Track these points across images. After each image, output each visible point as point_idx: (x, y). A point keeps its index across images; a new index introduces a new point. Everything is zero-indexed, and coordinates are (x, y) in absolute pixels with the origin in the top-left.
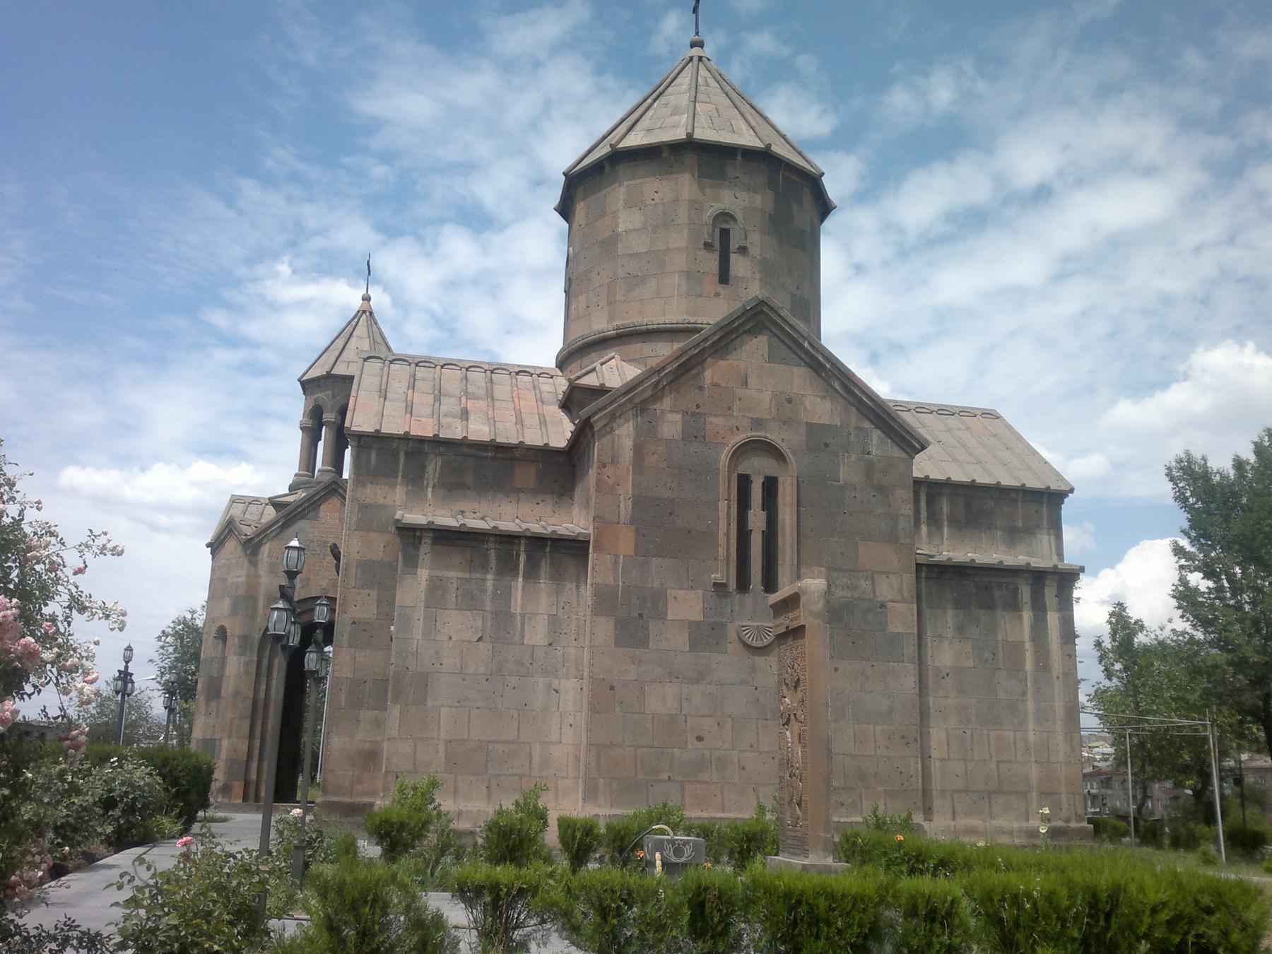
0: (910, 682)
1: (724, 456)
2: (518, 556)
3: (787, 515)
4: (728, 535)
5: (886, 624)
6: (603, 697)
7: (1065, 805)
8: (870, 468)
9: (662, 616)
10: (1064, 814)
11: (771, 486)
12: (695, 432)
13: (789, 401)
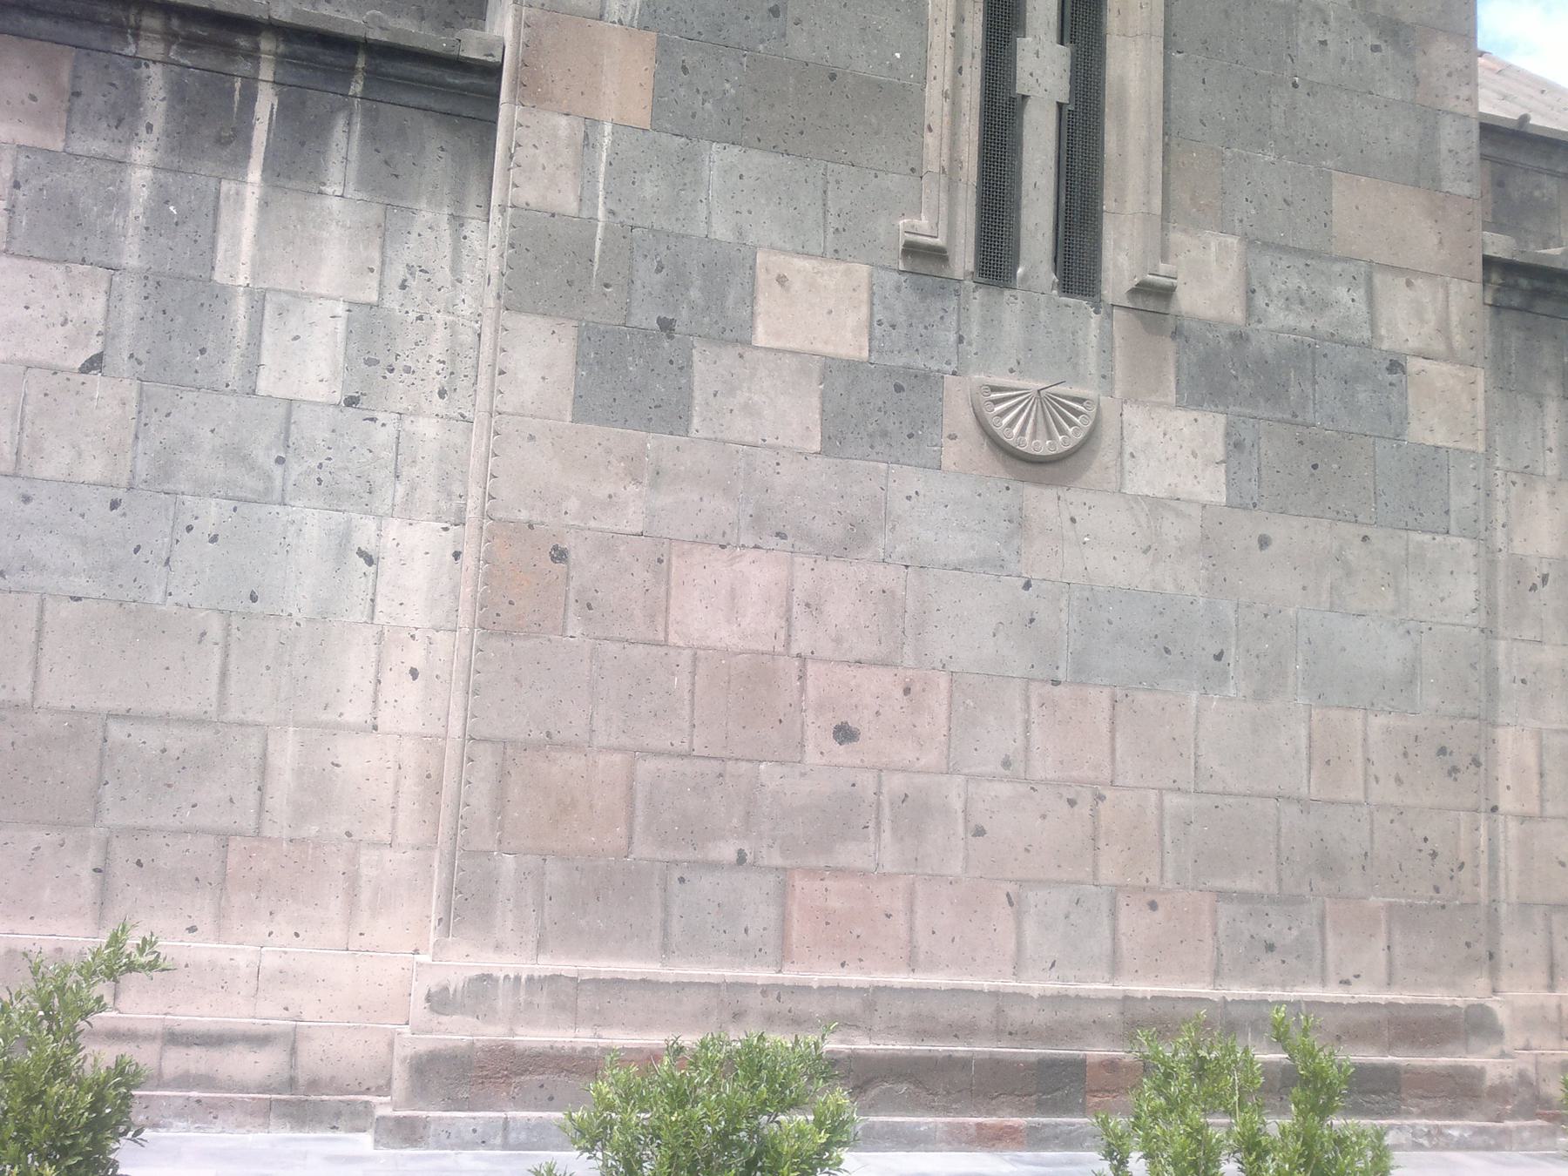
2: (250, 98)
3: (1132, 65)
4: (953, 96)
5: (1404, 418)
6: (523, 584)
9: (736, 335)
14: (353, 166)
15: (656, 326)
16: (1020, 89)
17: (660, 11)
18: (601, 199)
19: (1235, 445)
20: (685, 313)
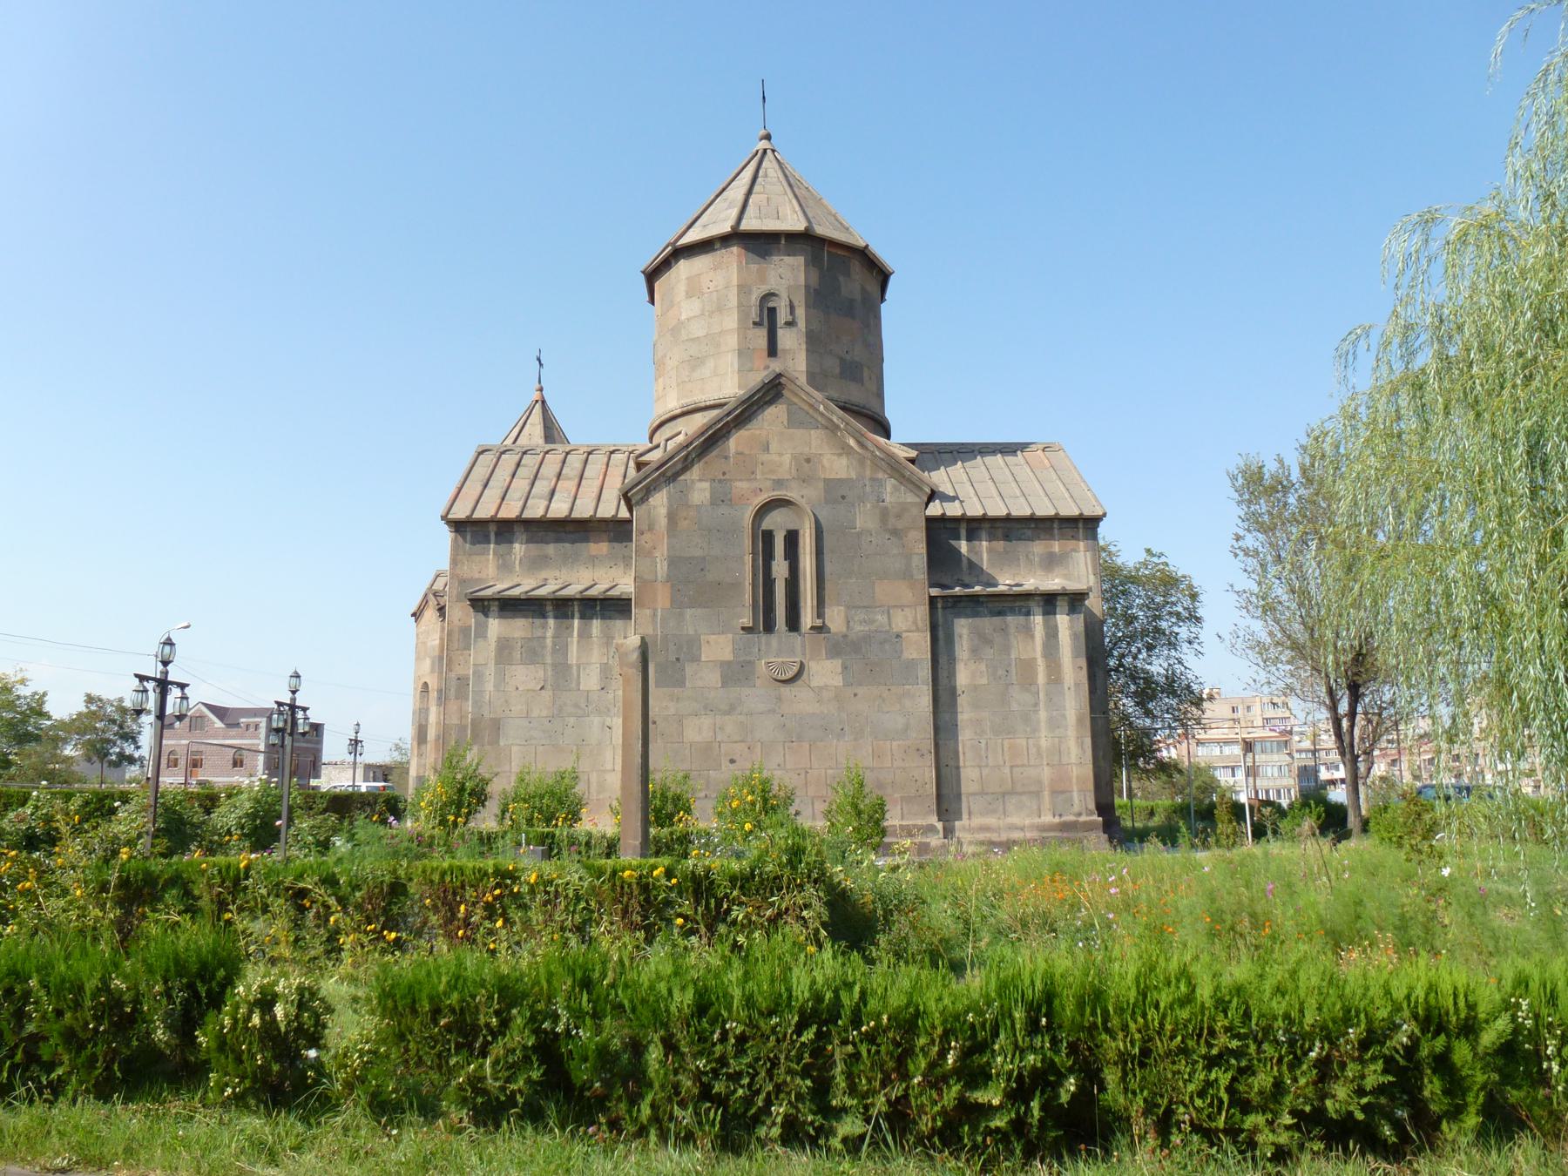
0: (925, 701)
1: (748, 515)
7: (1076, 801)
8: (884, 514)
9: (696, 659)
10: (1076, 809)
11: (792, 539)
13: (808, 461)
19: (845, 668)
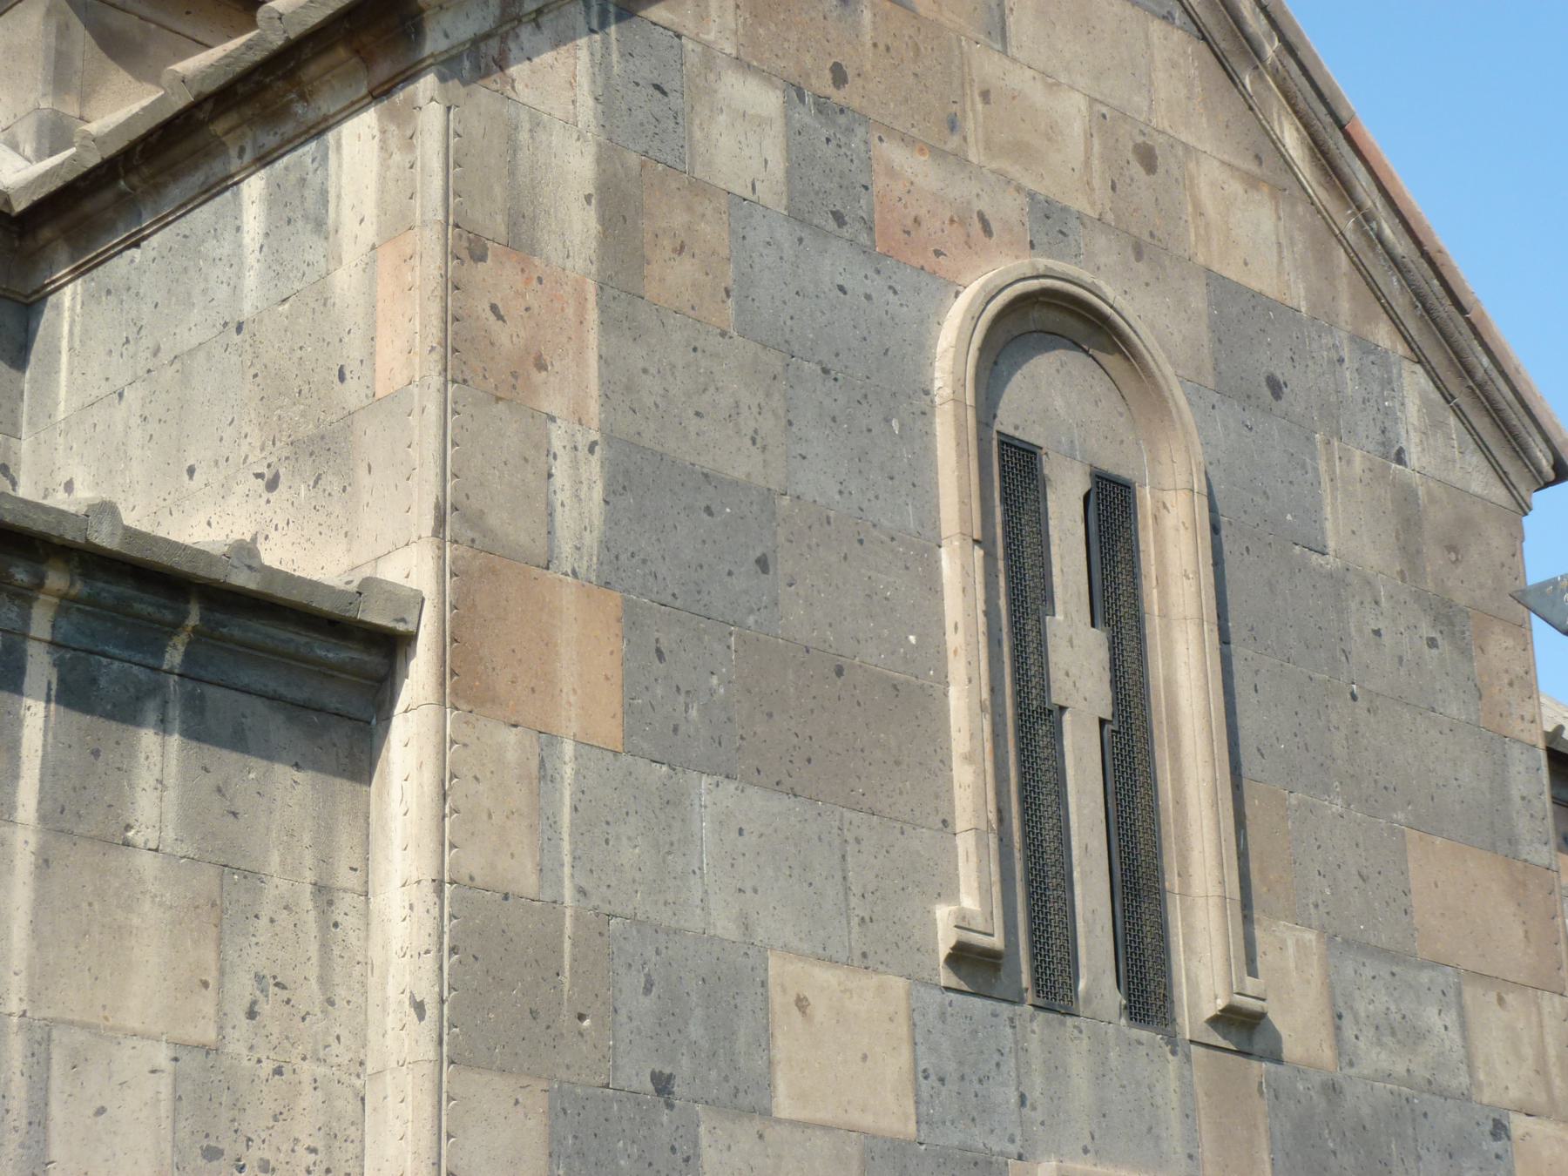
9: (748, 1100)
12: (830, 203)
13: (1148, 158)
14: (171, 795)
15: (650, 1087)
16: (1057, 698)
17: (623, 557)
18: (567, 870)
20: (685, 1061)
